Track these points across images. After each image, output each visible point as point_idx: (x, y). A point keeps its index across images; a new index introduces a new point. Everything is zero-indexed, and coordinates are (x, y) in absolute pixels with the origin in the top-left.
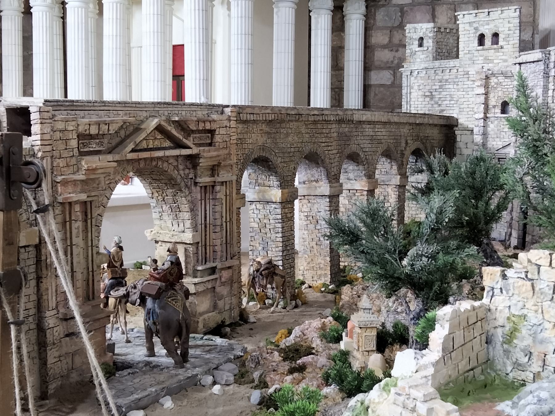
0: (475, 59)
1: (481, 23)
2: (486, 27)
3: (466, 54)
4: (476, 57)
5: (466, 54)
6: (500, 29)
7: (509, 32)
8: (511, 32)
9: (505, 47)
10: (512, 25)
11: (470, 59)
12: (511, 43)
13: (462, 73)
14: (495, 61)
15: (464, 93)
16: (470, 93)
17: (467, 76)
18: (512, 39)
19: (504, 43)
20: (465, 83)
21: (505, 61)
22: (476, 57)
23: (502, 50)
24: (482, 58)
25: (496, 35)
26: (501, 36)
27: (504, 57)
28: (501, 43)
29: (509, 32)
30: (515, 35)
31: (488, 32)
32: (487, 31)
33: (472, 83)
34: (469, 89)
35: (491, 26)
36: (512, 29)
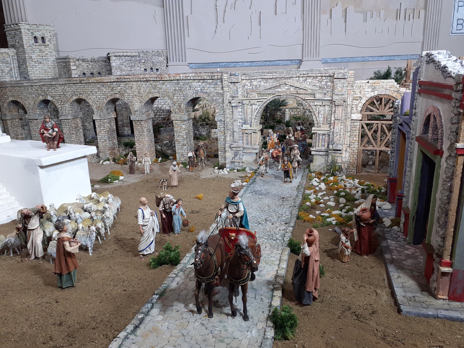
0: (34, 50)
1: (34, 30)
2: (38, 33)
3: (29, 46)
4: (35, 49)
5: (29, 46)
6: (46, 35)
7: (51, 38)
8: (52, 38)
9: (50, 45)
10: (51, 34)
11: (32, 50)
12: (52, 43)
13: (28, 57)
14: (46, 52)
15: (31, 69)
16: (34, 68)
17: (31, 59)
18: (52, 41)
19: (49, 43)
20: (31, 63)
21: (51, 52)
22: (35, 49)
23: (49, 47)
24: (38, 50)
25: (43, 38)
26: (47, 40)
27: (49, 50)
28: (47, 43)
29: (51, 38)
30: (54, 39)
31: (38, 35)
32: (39, 35)
33: (34, 63)
34: (33, 67)
35: (41, 33)
36: (52, 36)
